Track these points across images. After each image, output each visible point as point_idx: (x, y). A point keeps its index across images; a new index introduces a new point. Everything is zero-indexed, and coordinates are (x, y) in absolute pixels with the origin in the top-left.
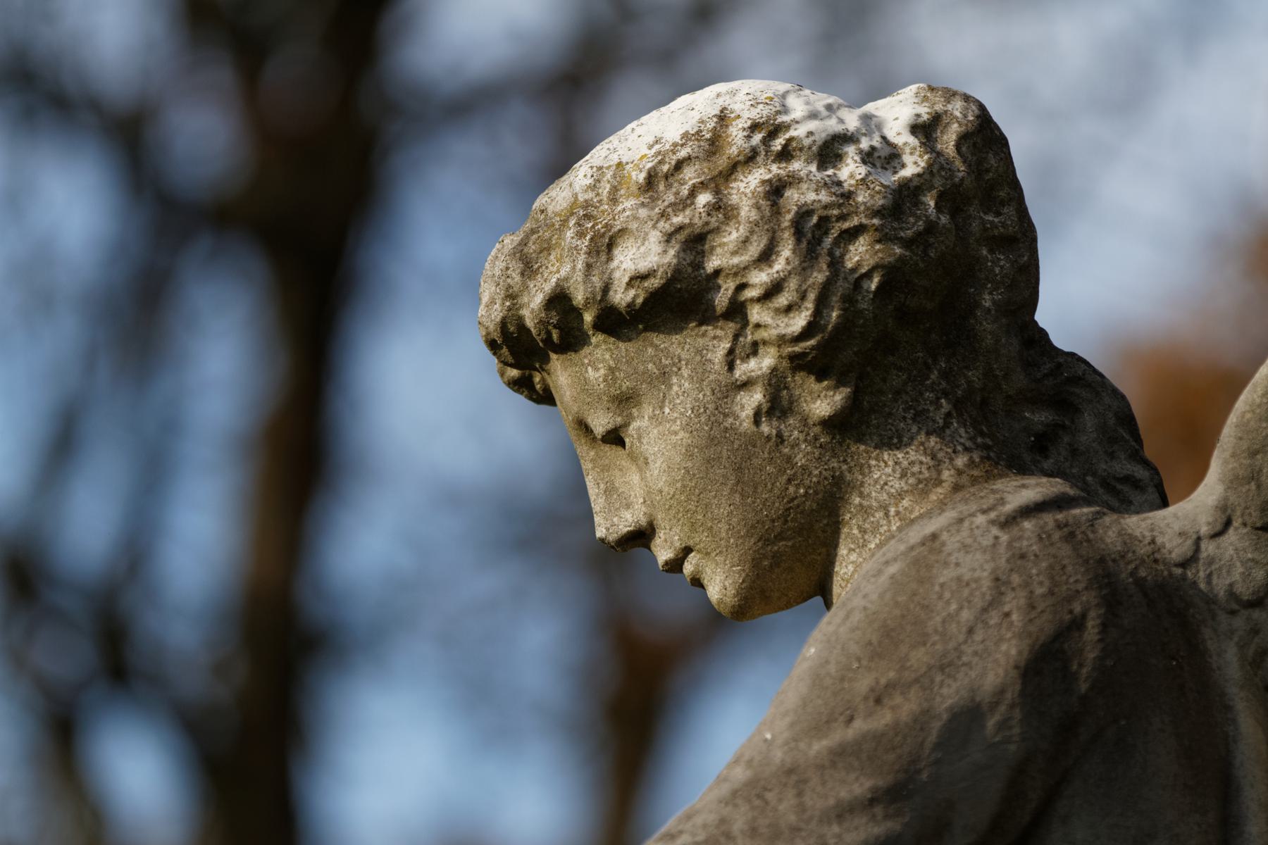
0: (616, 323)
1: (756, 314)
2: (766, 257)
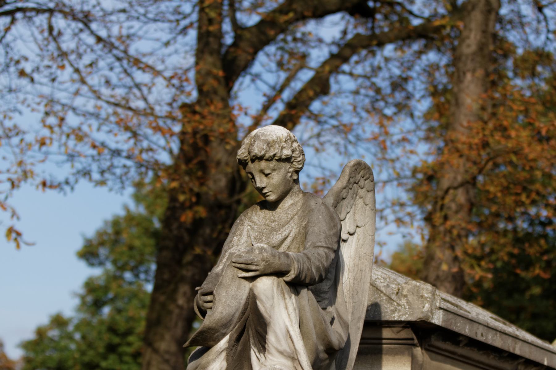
0: (280, 160)
1: (294, 163)
2: (299, 157)
